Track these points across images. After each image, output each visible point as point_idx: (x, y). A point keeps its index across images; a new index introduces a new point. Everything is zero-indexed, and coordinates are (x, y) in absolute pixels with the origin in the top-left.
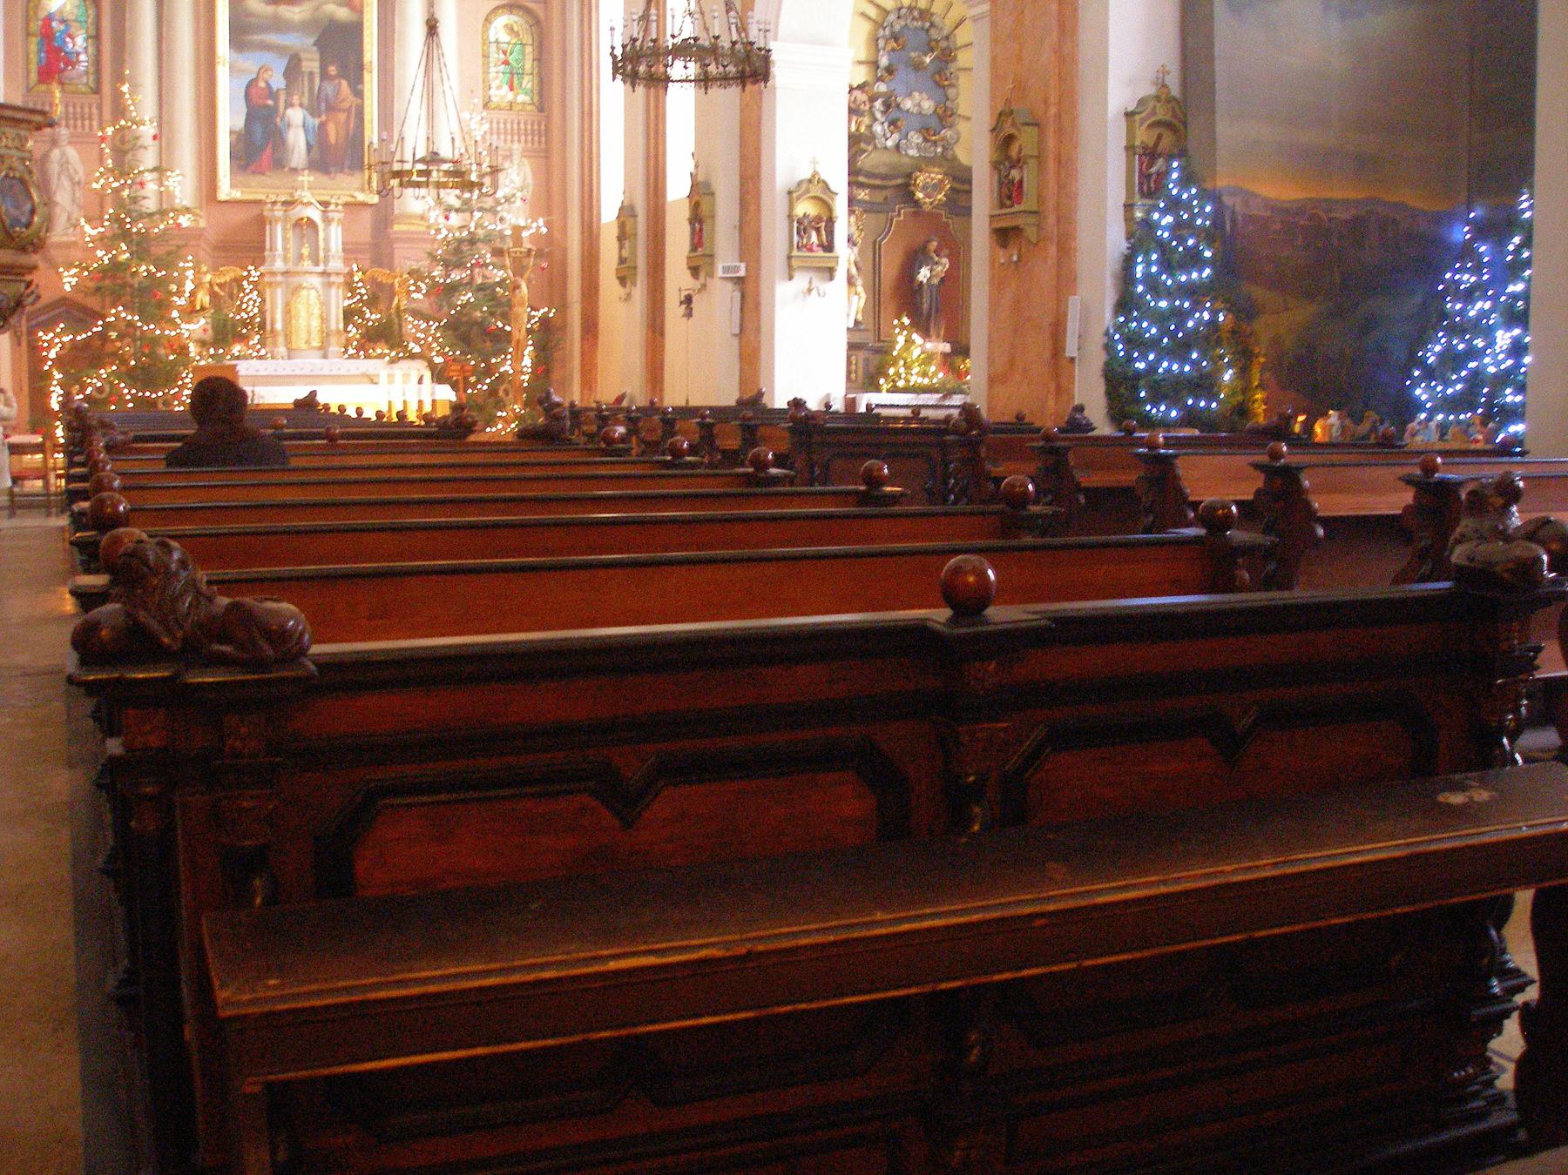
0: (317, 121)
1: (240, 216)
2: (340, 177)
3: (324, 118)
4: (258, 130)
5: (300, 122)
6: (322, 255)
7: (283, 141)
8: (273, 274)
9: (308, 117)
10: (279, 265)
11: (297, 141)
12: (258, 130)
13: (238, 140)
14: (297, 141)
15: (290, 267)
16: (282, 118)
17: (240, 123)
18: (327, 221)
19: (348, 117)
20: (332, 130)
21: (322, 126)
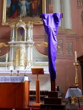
0: (29, 3)
1: (7, 30)
2: (36, 17)
3: (31, 2)
4: (14, 7)
5: (25, 4)
6: (25, 38)
7: (20, 9)
8: (11, 44)
9: (27, 3)
10: (13, 41)
11: (24, 9)
12: (14, 7)
13: (9, 10)
14: (24, 9)
15: (17, 42)
16: (20, 4)
17: (9, 6)
18: (27, 28)
19: (38, 2)
20: (33, 5)
21: (31, 4)
